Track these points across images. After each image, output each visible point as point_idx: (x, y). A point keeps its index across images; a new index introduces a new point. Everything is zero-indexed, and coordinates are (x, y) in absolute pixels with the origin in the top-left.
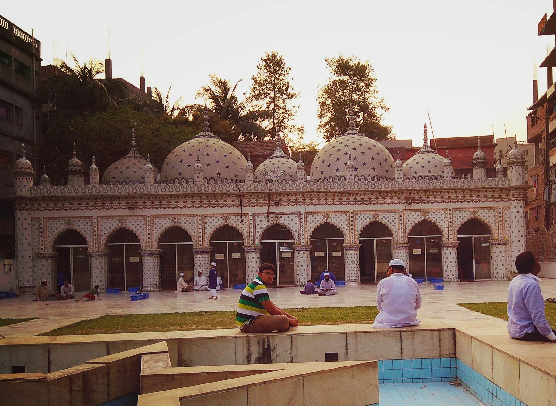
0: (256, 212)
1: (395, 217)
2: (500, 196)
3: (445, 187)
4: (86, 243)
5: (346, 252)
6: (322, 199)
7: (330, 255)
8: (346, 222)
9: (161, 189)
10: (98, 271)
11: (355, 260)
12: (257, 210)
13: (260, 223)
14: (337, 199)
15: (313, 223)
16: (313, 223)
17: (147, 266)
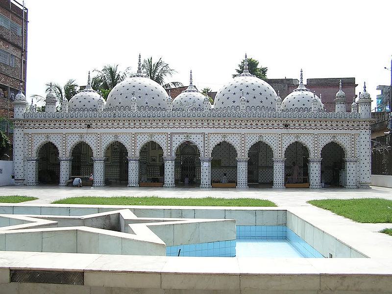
6: (222, 124)
8: (239, 141)
10: (64, 171)
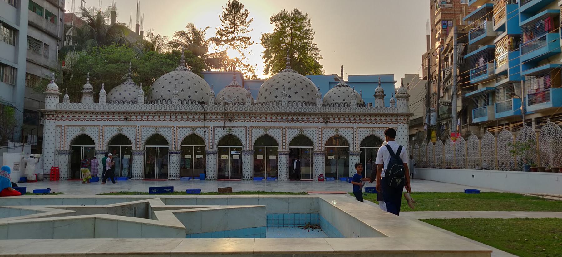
0: (215, 125)
1: (315, 132)
2: (391, 120)
3: (352, 112)
4: (94, 144)
5: (279, 156)
6: (263, 118)
7: (268, 158)
8: (280, 135)
9: (149, 108)
11: (285, 162)
12: (216, 124)
13: (218, 133)
14: (274, 118)
15: (256, 135)
16: (256, 135)
17: (135, 162)
